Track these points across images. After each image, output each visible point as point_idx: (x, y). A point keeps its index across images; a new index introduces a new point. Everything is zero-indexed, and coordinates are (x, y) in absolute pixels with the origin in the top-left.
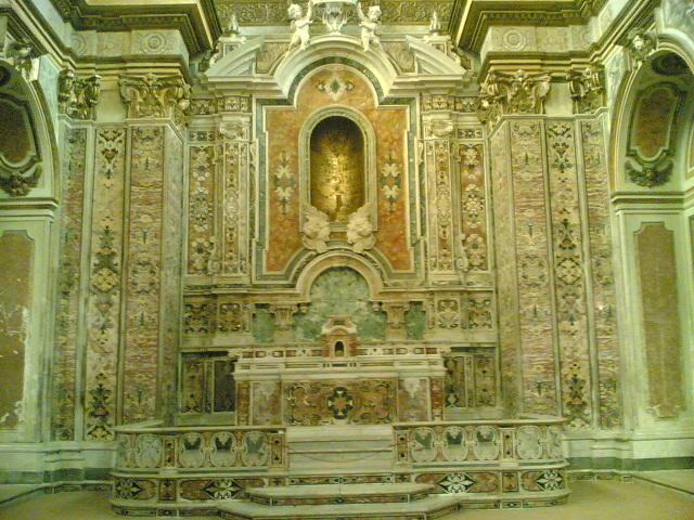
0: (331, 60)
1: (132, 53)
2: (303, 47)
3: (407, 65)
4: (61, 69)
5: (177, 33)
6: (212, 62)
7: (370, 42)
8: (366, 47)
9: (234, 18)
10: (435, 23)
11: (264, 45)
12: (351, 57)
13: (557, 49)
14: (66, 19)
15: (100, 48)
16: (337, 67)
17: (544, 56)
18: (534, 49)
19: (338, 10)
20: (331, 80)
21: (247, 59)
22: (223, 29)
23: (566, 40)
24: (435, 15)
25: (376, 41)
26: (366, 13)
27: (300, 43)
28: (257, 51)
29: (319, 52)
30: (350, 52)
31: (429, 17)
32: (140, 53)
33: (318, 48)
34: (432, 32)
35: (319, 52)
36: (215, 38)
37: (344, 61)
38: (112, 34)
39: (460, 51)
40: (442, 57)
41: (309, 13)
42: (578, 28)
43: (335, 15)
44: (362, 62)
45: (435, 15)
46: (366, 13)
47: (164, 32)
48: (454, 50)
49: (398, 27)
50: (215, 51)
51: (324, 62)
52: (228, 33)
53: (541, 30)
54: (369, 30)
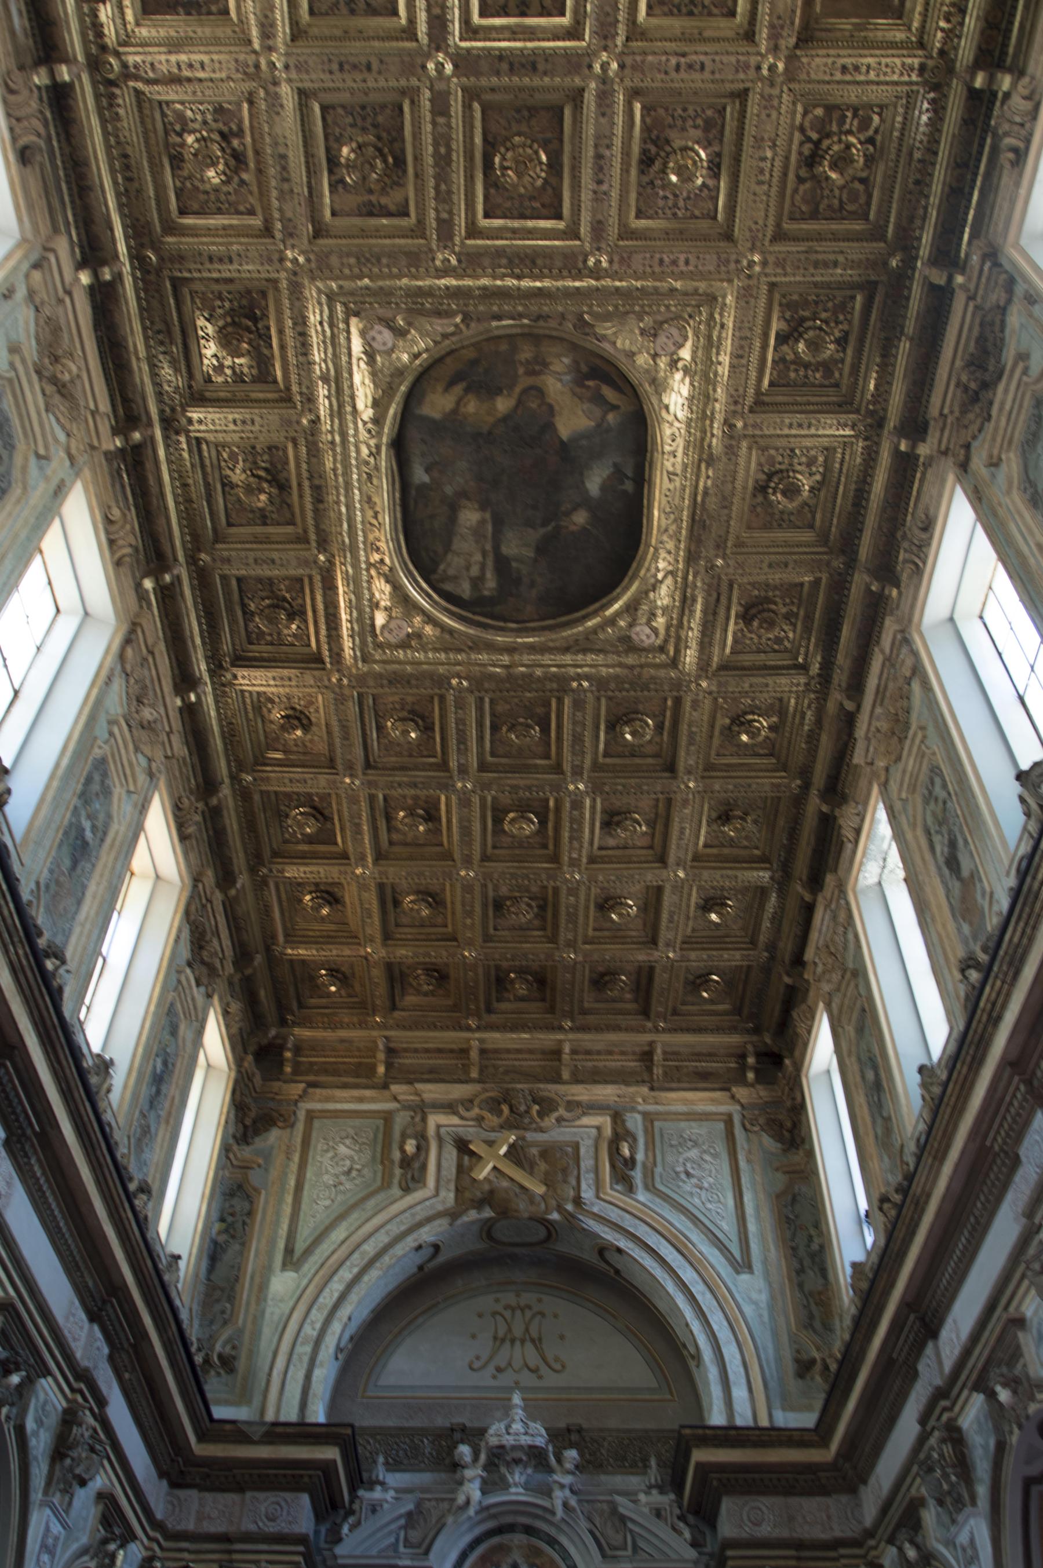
0: (511, 1528)
1: (243, 1528)
2: (471, 1512)
3: (617, 1539)
4: (145, 1553)
5: (305, 1499)
6: (345, 1529)
7: (565, 1505)
8: (560, 1512)
9: (381, 1459)
10: (654, 1474)
11: (419, 1504)
12: (539, 1524)
13: (819, 1534)
14: (162, 1474)
15: (200, 1517)
16: (518, 1539)
17: (800, 1545)
18: (785, 1533)
19: (519, 1455)
20: (510, 1561)
21: (393, 1526)
22: (365, 1475)
23: (829, 1517)
24: (653, 1462)
25: (573, 1502)
26: (559, 1461)
27: (468, 1502)
28: (409, 1515)
29: (494, 1516)
30: (537, 1517)
31: (645, 1460)
32: (253, 1527)
33: (493, 1511)
34: (650, 1487)
35: (494, 1516)
36: (353, 1490)
37: (529, 1530)
38: (219, 1496)
39: (691, 1518)
40: (662, 1530)
41: (483, 1457)
42: (844, 1498)
43: (517, 1462)
44: (553, 1532)
45: (653, 1462)
46: (559, 1461)
47: (288, 1496)
48: (682, 1518)
49: (603, 1478)
50: (352, 1512)
51: (499, 1531)
52: (371, 1485)
53: (794, 1501)
54: (562, 1486)
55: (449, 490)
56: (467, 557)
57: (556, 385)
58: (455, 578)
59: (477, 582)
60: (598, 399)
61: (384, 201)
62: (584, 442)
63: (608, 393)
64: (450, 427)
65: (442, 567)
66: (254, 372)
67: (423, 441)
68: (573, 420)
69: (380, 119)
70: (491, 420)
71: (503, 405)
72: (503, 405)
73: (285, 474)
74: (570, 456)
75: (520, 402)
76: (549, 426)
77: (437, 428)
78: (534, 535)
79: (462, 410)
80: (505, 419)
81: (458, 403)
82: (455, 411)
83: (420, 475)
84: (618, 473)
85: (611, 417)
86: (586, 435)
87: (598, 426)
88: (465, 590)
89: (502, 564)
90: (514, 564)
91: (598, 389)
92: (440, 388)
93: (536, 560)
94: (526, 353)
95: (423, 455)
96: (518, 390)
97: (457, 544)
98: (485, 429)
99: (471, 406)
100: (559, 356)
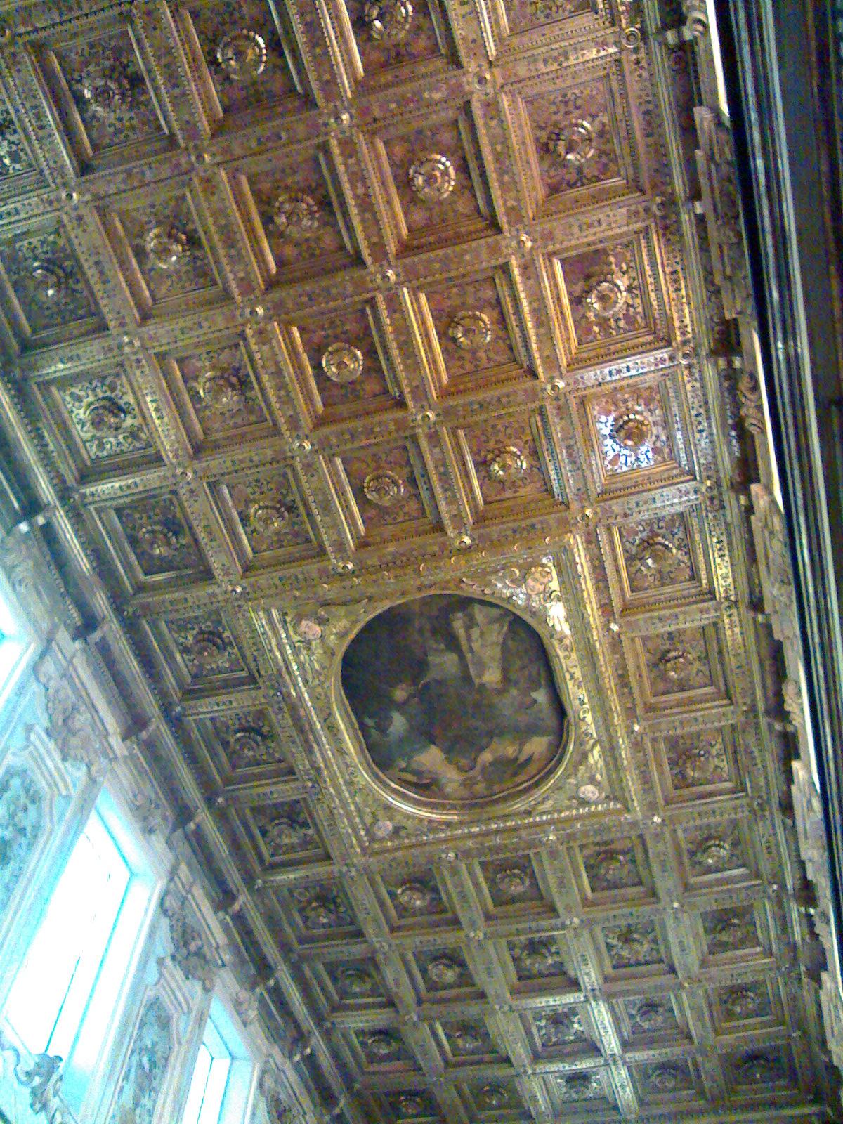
56: (485, 645)
57: (452, 778)
58: (491, 622)
59: (471, 623)
62: (417, 746)
64: (524, 733)
65: (505, 628)
68: (431, 758)
70: (494, 745)
72: (487, 757)
73: (653, 675)
74: (425, 734)
75: (475, 760)
76: (448, 751)
77: (534, 729)
79: (517, 747)
80: (482, 749)
81: (520, 751)
82: (522, 745)
83: (541, 696)
84: (383, 730)
85: (403, 765)
86: (418, 751)
89: (452, 643)
90: (442, 646)
92: (536, 756)
95: (540, 711)
96: (478, 767)
97: (497, 652)
98: (495, 739)
99: (510, 751)
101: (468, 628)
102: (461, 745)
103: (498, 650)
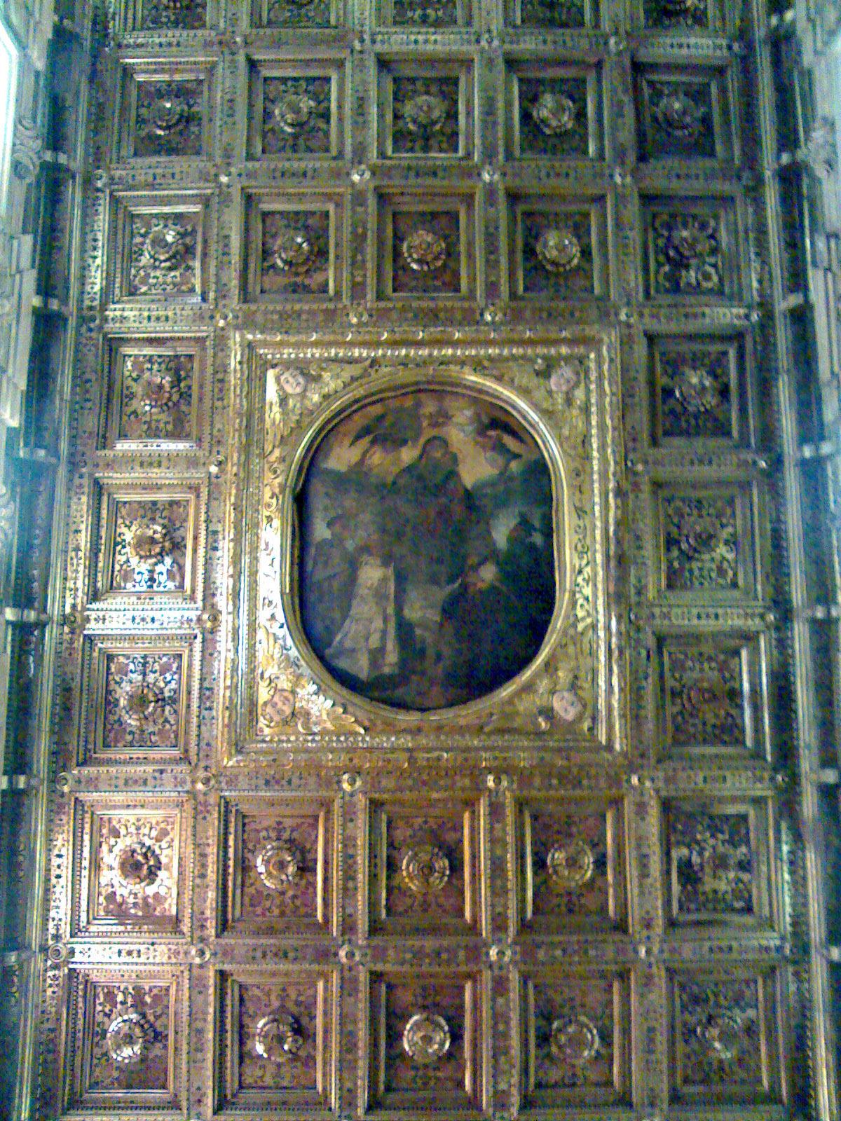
55: (350, 545)
57: (460, 433)
59: (377, 655)
60: (500, 448)
61: (307, 282)
62: (489, 491)
63: (508, 441)
65: (338, 638)
66: (170, 427)
67: (327, 494)
68: (477, 469)
69: (310, 222)
70: (396, 470)
71: (408, 455)
72: (408, 455)
76: (453, 474)
77: (341, 481)
78: (441, 594)
79: (368, 462)
80: (408, 470)
81: (364, 454)
82: (362, 461)
83: (321, 531)
85: (515, 466)
87: (502, 474)
88: (361, 667)
89: (405, 631)
90: (418, 632)
91: (500, 440)
92: (347, 442)
93: (441, 625)
94: (430, 407)
95: (326, 509)
96: (422, 441)
98: (390, 479)
100: (461, 410)
101: (382, 650)
102: (434, 481)
103: (352, 612)
